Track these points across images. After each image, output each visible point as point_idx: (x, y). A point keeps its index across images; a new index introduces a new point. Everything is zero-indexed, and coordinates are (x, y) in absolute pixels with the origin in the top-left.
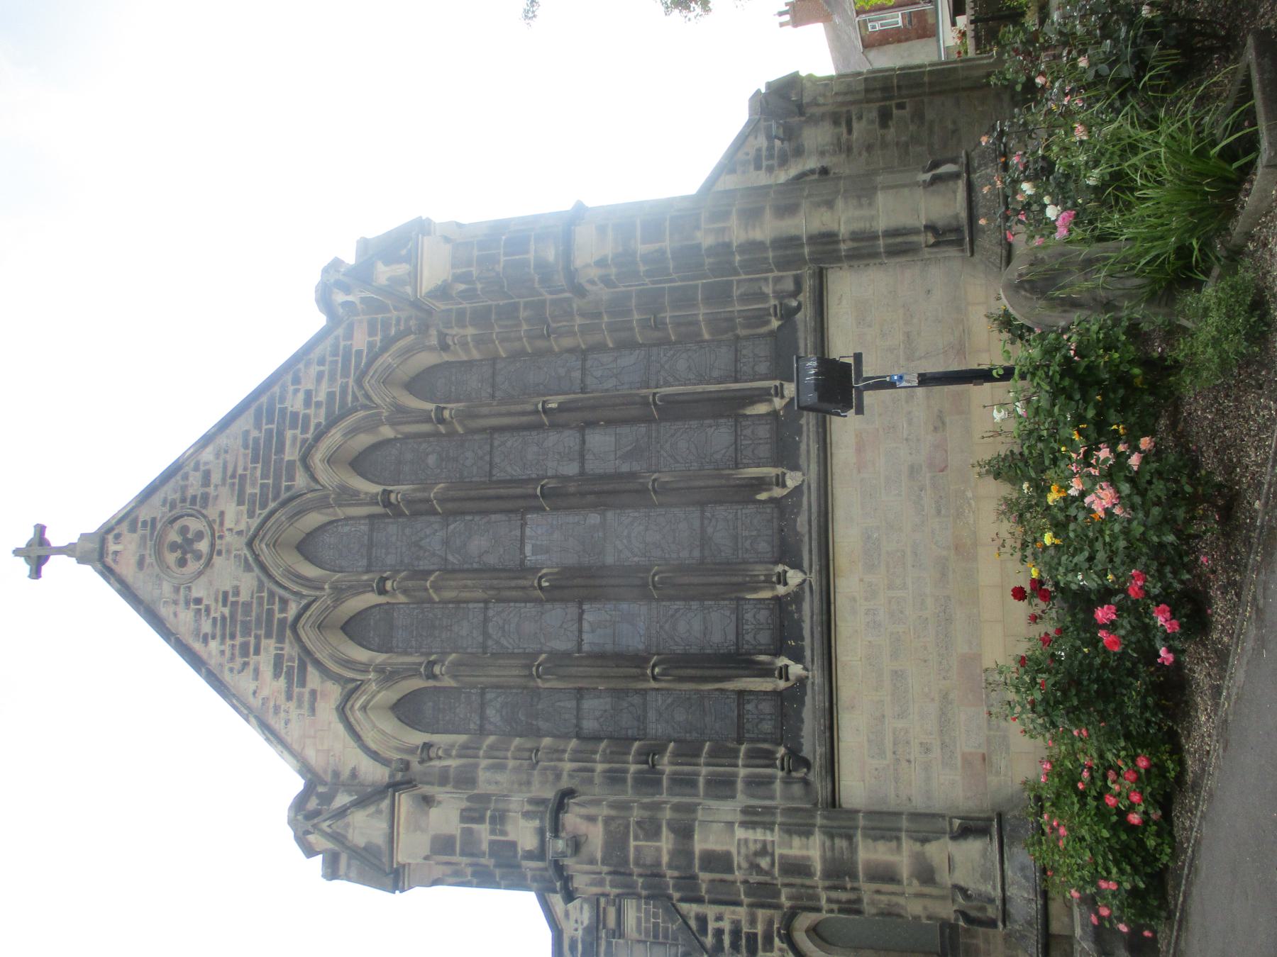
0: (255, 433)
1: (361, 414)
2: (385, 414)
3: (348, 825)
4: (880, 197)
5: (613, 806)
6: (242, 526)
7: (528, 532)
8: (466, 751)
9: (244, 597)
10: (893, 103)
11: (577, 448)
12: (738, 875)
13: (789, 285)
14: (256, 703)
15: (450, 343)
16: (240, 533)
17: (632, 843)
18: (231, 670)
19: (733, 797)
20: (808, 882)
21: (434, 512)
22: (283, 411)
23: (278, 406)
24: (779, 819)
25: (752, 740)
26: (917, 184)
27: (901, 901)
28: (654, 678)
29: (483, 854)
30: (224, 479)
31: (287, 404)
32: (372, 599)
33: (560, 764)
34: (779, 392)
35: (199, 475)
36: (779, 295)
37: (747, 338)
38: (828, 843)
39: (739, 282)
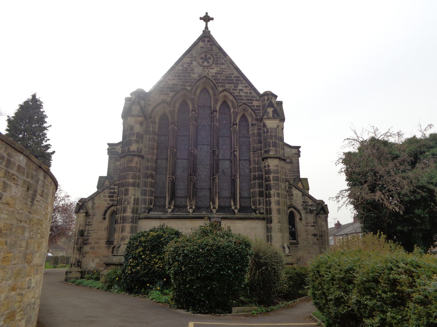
0: (233, 76)
1: (236, 104)
2: (236, 110)
4: (280, 234)
5: (140, 168)
6: (210, 74)
7: (206, 146)
9: (192, 75)
10: (319, 238)
11: (225, 158)
12: (124, 197)
13: (261, 211)
15: (253, 127)
16: (208, 74)
17: (131, 173)
18: (175, 73)
19: (142, 195)
20: (122, 212)
21: (211, 123)
22: (238, 84)
23: (240, 82)
24: (136, 206)
25: (155, 200)
26: (283, 243)
27: (118, 233)
28: (169, 177)
30: (222, 69)
31: (240, 85)
32: (191, 108)
33: (150, 155)
34: (236, 208)
35: (223, 62)
36: (260, 208)
37: (250, 201)
38: (130, 217)
39: (263, 199)
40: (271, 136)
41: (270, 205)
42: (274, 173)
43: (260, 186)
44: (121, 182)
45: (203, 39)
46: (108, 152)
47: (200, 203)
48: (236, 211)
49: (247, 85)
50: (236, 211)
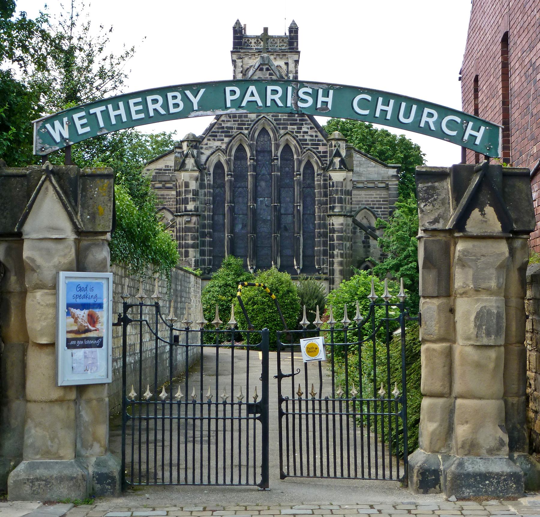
1: (300, 151)
2: (300, 158)
3: (190, 158)
5: (198, 227)
13: (325, 271)
22: (302, 124)
31: (305, 126)
32: (249, 155)
34: (298, 268)
40: (337, 190)
41: (333, 266)
42: (339, 232)
43: (325, 244)
45: (261, 67)
47: (261, 262)
48: (299, 271)
49: (313, 126)
50: (299, 271)
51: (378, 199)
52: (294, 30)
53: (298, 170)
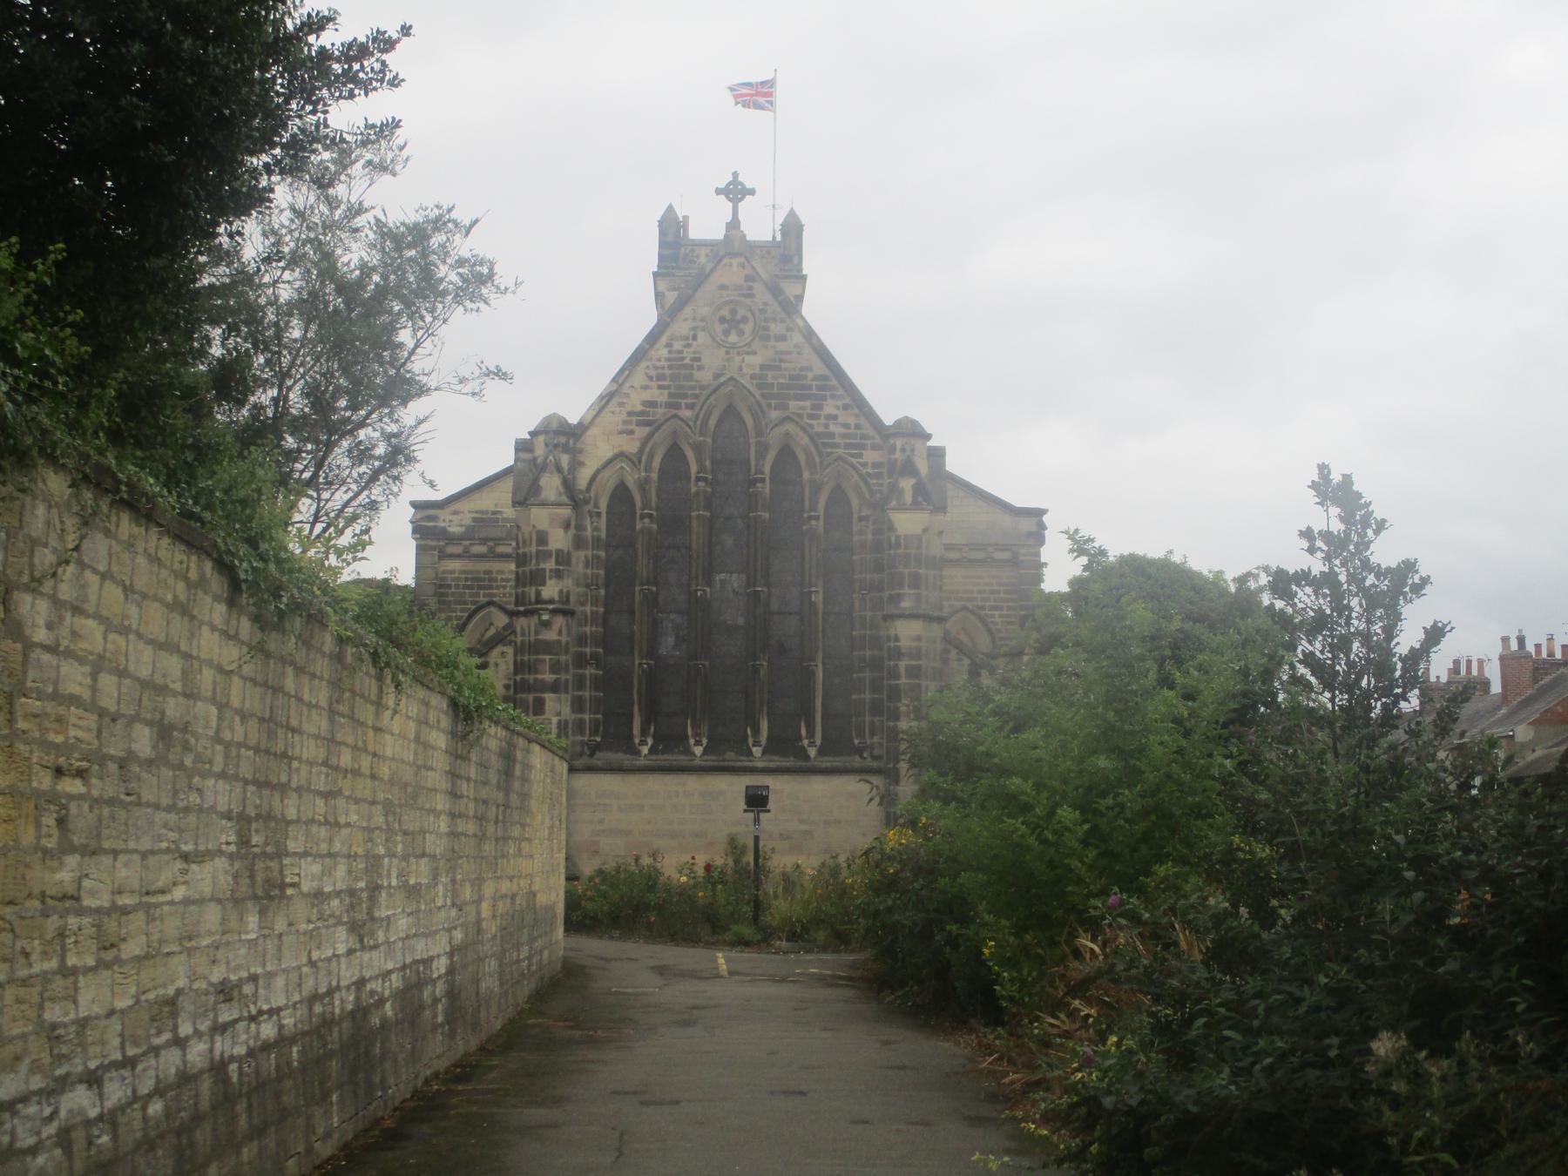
0: (810, 375)
2: (817, 477)
3: (551, 473)
5: (567, 643)
6: (745, 370)
8: (597, 540)
9: (697, 374)
13: (877, 752)
14: (626, 389)
16: (741, 368)
17: (547, 657)
18: (648, 367)
22: (824, 398)
28: (640, 664)
29: (537, 564)
31: (830, 401)
32: (694, 468)
36: (872, 747)
44: (522, 679)
46: (415, 531)
48: (812, 752)
51: (996, 588)
52: (793, 229)
53: (813, 507)
